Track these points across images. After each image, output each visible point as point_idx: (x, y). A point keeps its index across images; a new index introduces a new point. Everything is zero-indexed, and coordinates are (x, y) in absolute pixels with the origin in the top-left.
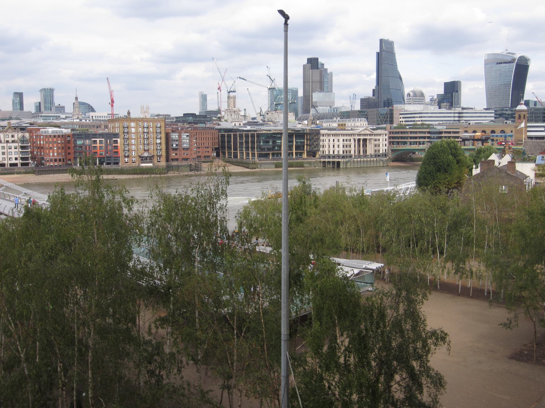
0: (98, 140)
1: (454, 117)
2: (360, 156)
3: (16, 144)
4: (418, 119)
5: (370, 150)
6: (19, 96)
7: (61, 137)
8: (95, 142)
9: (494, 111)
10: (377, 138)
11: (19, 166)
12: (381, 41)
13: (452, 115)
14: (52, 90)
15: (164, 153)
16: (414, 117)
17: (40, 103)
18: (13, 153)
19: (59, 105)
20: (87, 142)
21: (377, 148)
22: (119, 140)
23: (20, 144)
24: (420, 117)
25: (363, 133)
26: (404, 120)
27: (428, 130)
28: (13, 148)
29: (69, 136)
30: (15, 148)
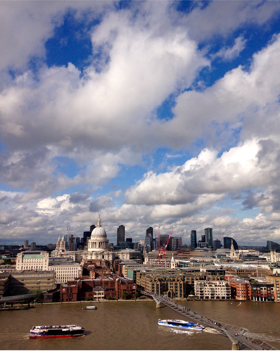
0: (263, 288)
3: (224, 287)
6: (194, 232)
7: (245, 285)
8: (262, 289)
11: (226, 298)
14: (211, 230)
17: (204, 236)
18: (223, 292)
19: (217, 240)
20: (258, 289)
22: (274, 288)
23: (226, 287)
28: (223, 289)
29: (248, 284)
30: (224, 289)
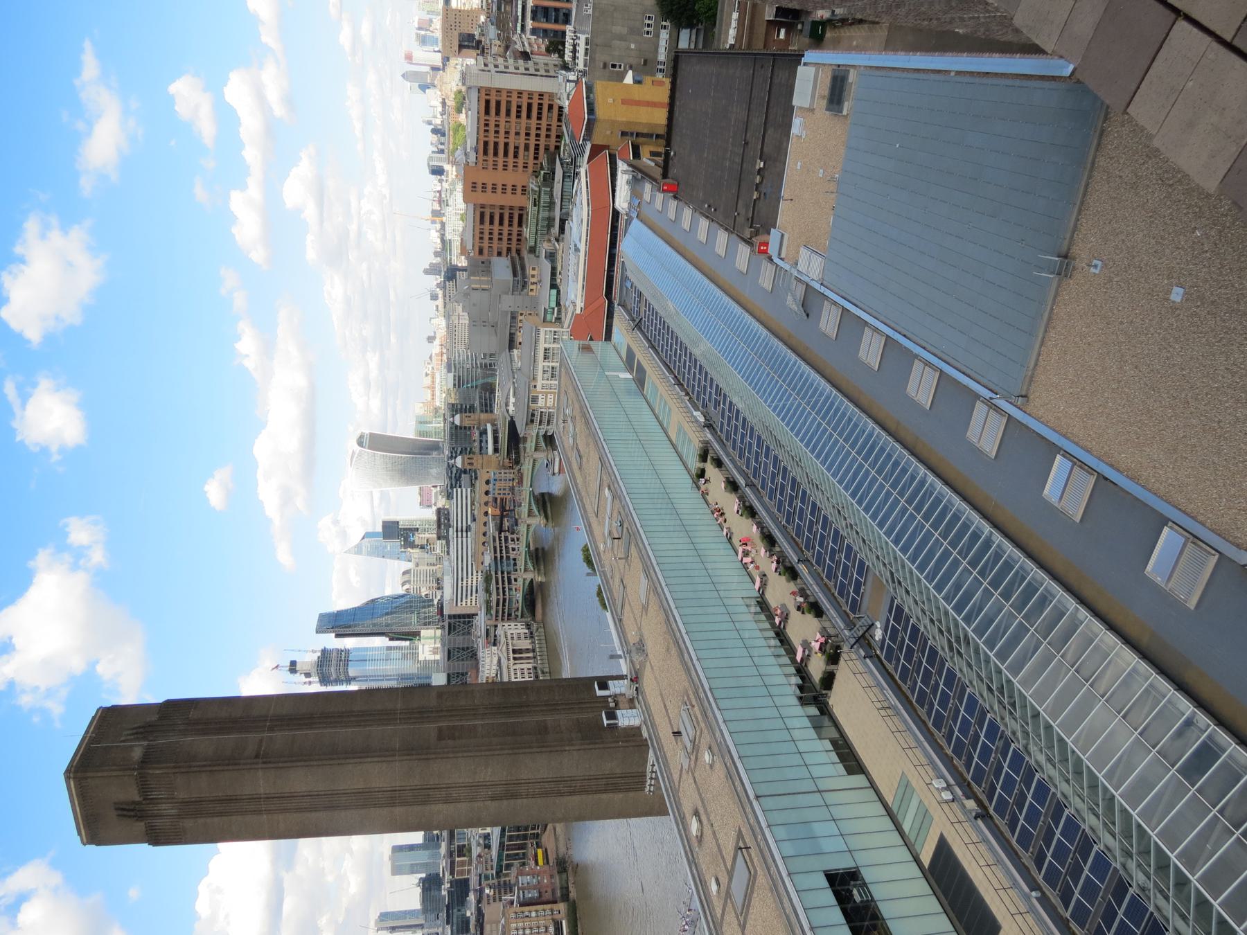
1: (462, 537)
2: (535, 657)
4: (465, 583)
5: (526, 644)
9: (455, 490)
10: (509, 636)
12: (317, 632)
13: (460, 540)
15: (549, 906)
16: (462, 587)
21: (522, 636)
24: (462, 580)
25: (505, 654)
26: (464, 600)
27: (493, 573)
